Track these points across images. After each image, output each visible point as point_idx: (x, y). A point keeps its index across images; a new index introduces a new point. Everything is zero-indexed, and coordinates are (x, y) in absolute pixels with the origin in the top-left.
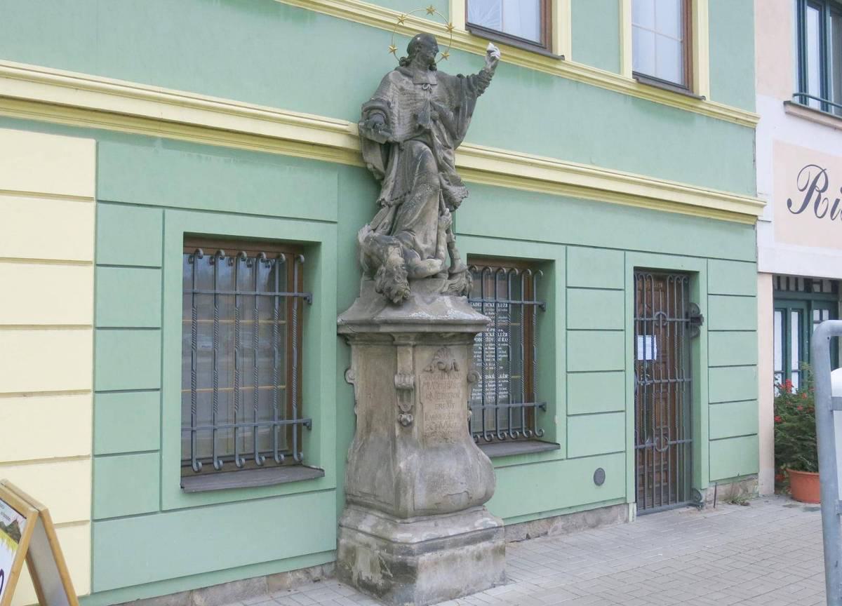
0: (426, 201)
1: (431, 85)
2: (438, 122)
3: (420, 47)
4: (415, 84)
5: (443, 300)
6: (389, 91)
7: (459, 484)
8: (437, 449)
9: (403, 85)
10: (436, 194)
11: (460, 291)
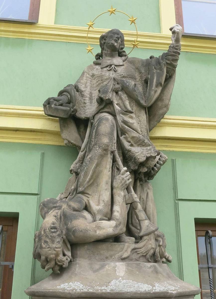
0: (96, 162)
1: (116, 66)
2: (120, 93)
3: (105, 40)
4: (102, 68)
5: (115, 267)
6: (83, 79)
9: (93, 72)
10: (106, 155)
11: (148, 256)
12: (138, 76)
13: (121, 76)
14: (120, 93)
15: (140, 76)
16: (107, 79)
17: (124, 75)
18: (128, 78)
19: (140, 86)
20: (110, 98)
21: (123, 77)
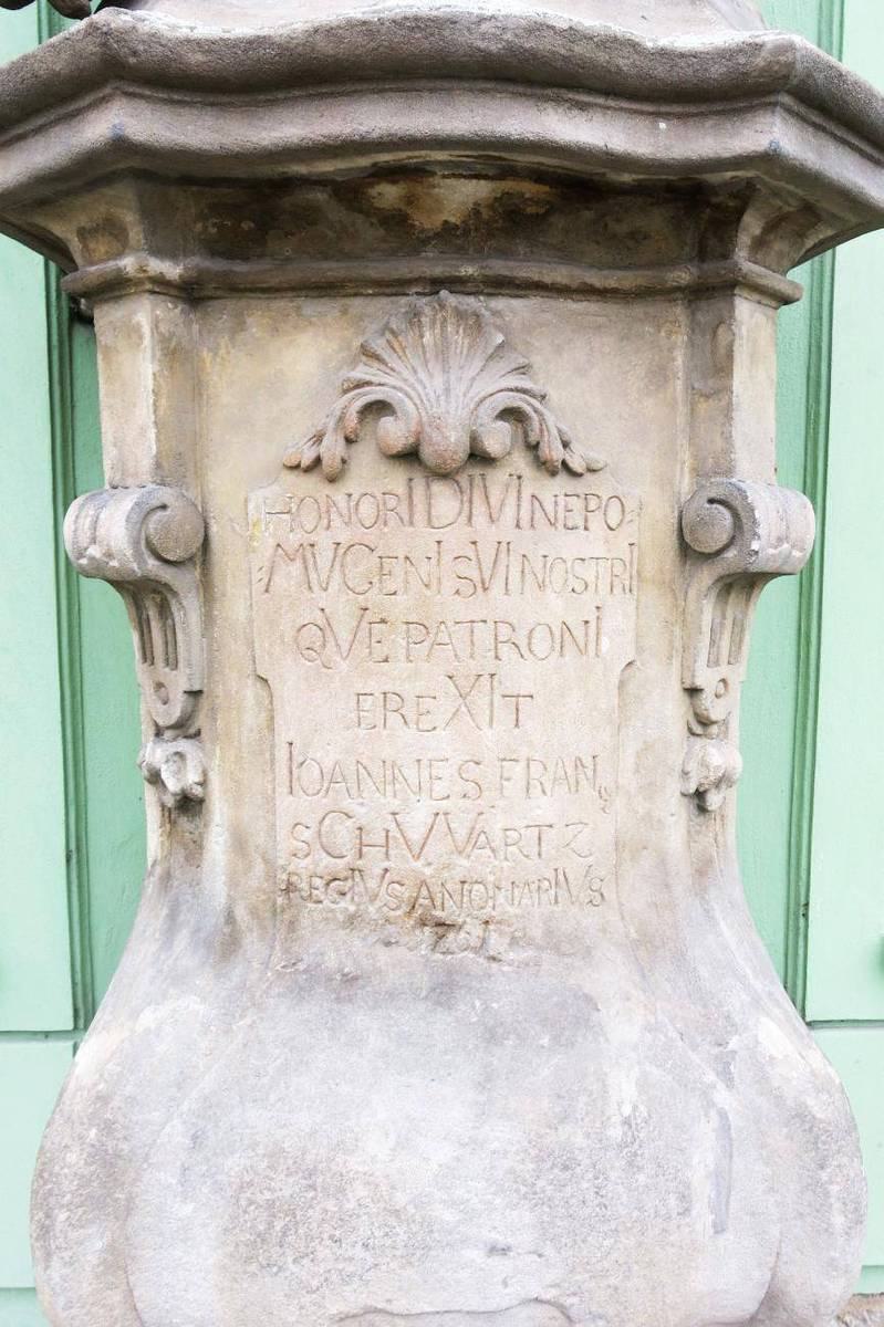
7: (476, 1255)
8: (349, 983)
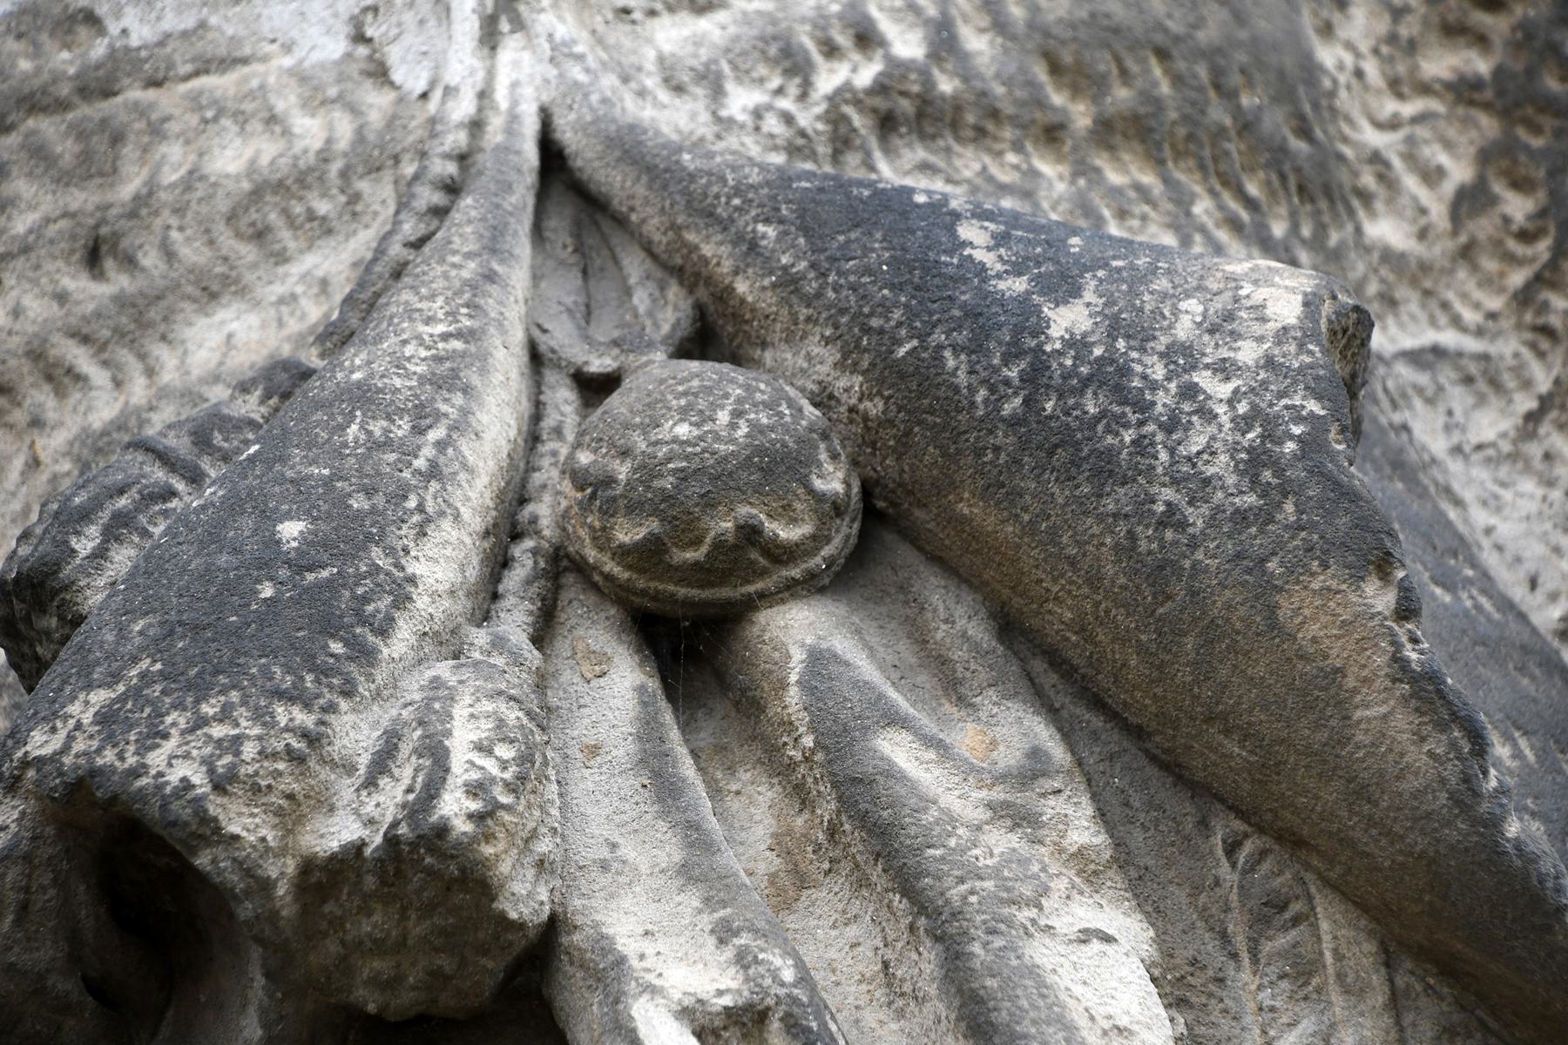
12: (1395, 87)
13: (795, 66)
14: (818, 659)
15: (1464, 91)
16: (304, 178)
17: (908, 45)
18: (1052, 134)
19: (1491, 425)
20: (454, 806)
21: (887, 124)
